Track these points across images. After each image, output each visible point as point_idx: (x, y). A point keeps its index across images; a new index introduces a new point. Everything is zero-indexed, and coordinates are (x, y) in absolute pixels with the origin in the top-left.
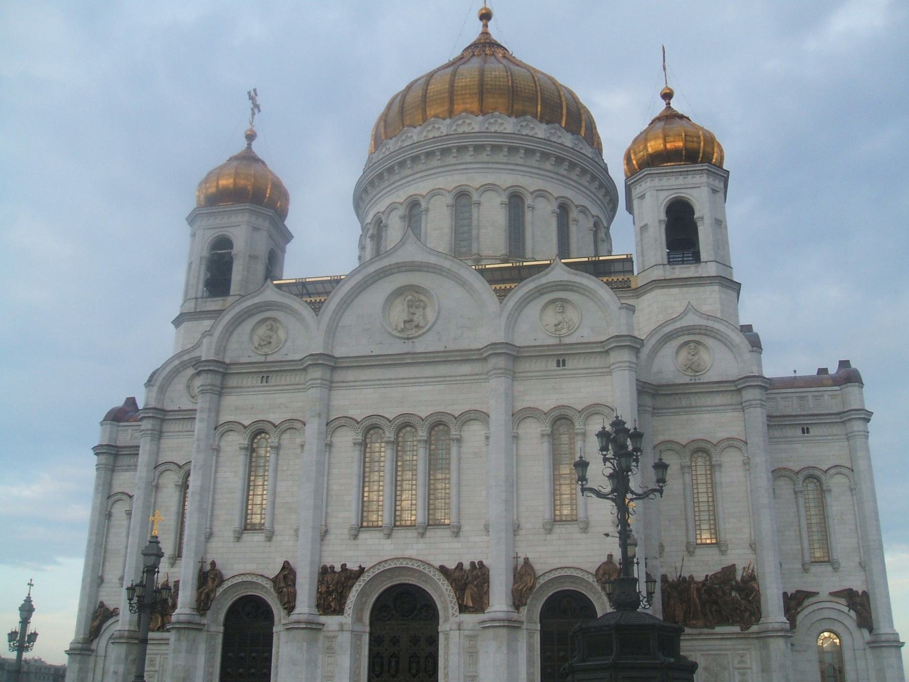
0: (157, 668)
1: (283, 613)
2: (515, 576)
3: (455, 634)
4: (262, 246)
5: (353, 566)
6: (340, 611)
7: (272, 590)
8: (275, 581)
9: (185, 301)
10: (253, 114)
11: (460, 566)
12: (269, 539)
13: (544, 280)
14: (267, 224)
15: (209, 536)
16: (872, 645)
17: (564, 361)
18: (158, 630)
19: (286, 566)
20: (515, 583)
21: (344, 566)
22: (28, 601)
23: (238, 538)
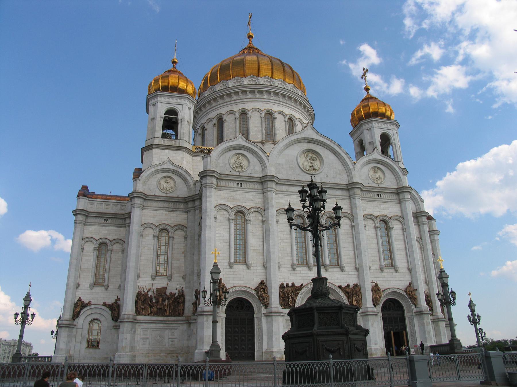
0: (148, 336)
1: (263, 307)
2: (372, 291)
5: (297, 284)
7: (255, 295)
8: (256, 290)
11: (348, 286)
12: (248, 268)
13: (371, 157)
17: (380, 195)
18: (148, 315)
19: (262, 283)
20: (373, 295)
21: (293, 284)
22: (28, 295)
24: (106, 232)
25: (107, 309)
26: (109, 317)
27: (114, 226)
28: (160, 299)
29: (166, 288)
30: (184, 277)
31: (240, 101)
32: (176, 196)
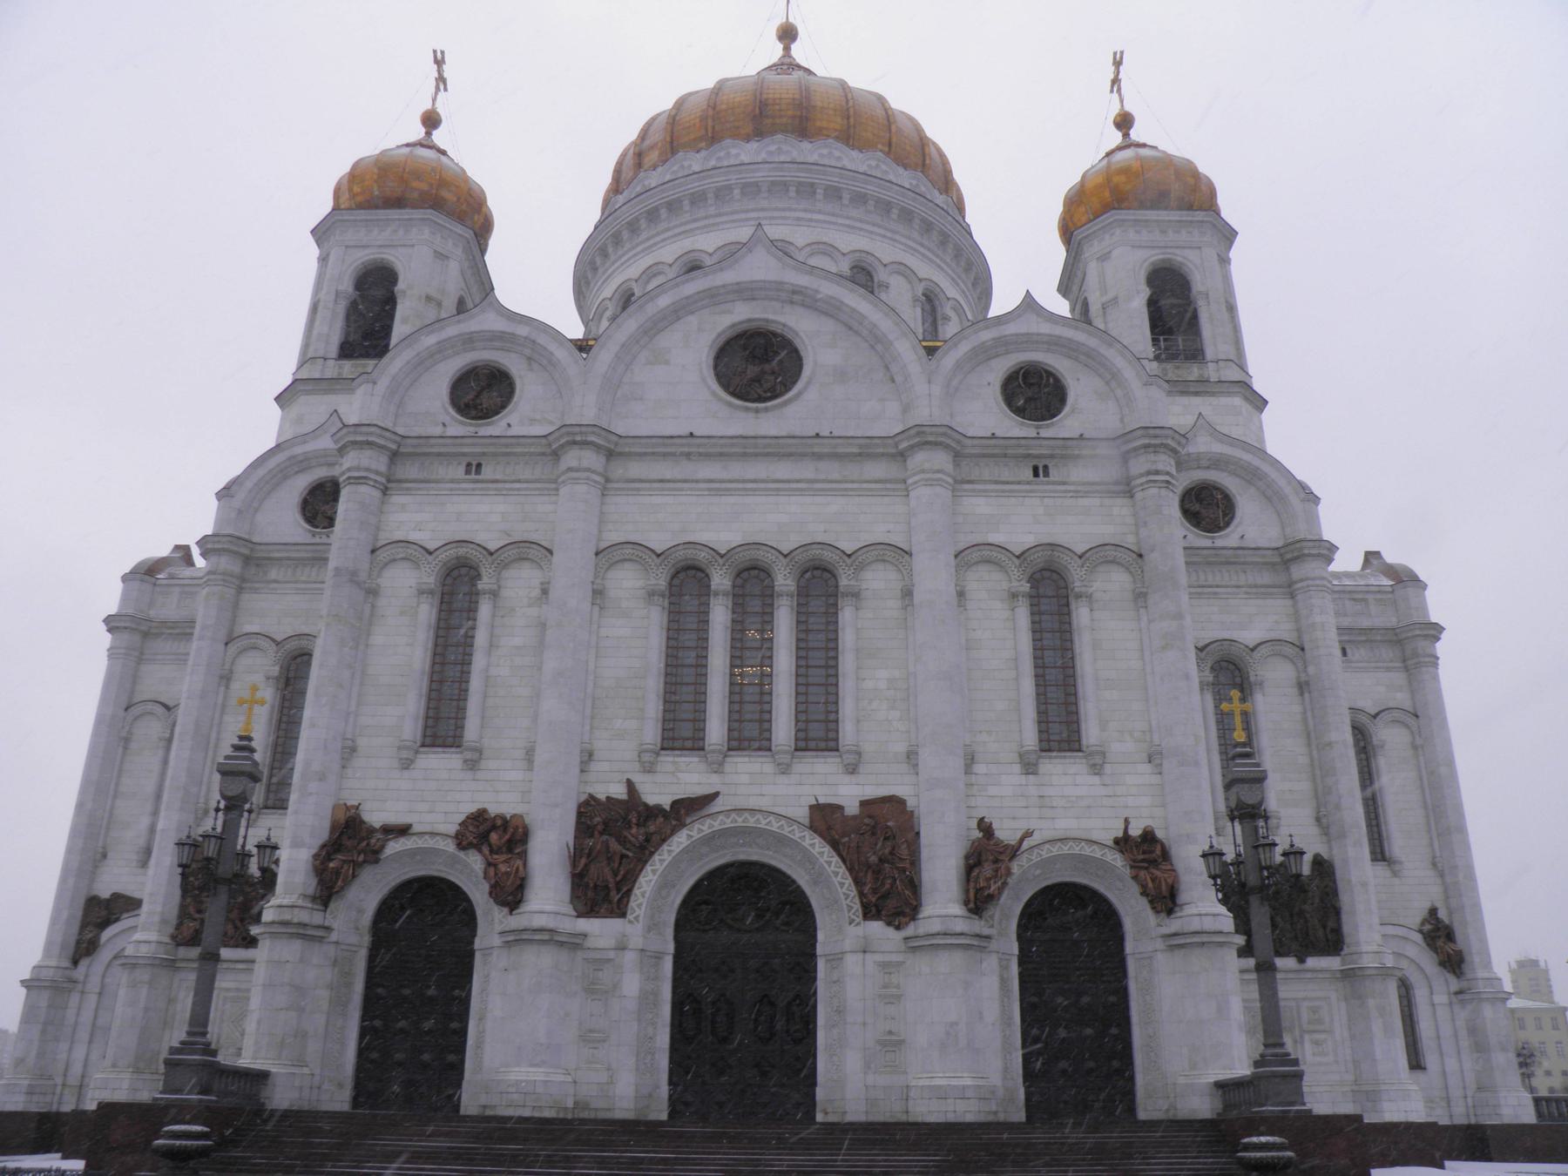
3: (852, 963)
4: (452, 281)
6: (620, 911)
9: (301, 365)
10: (438, 89)
12: (472, 765)
14: (459, 252)
15: (350, 751)
16: (1460, 997)
17: (1046, 467)
23: (407, 765)
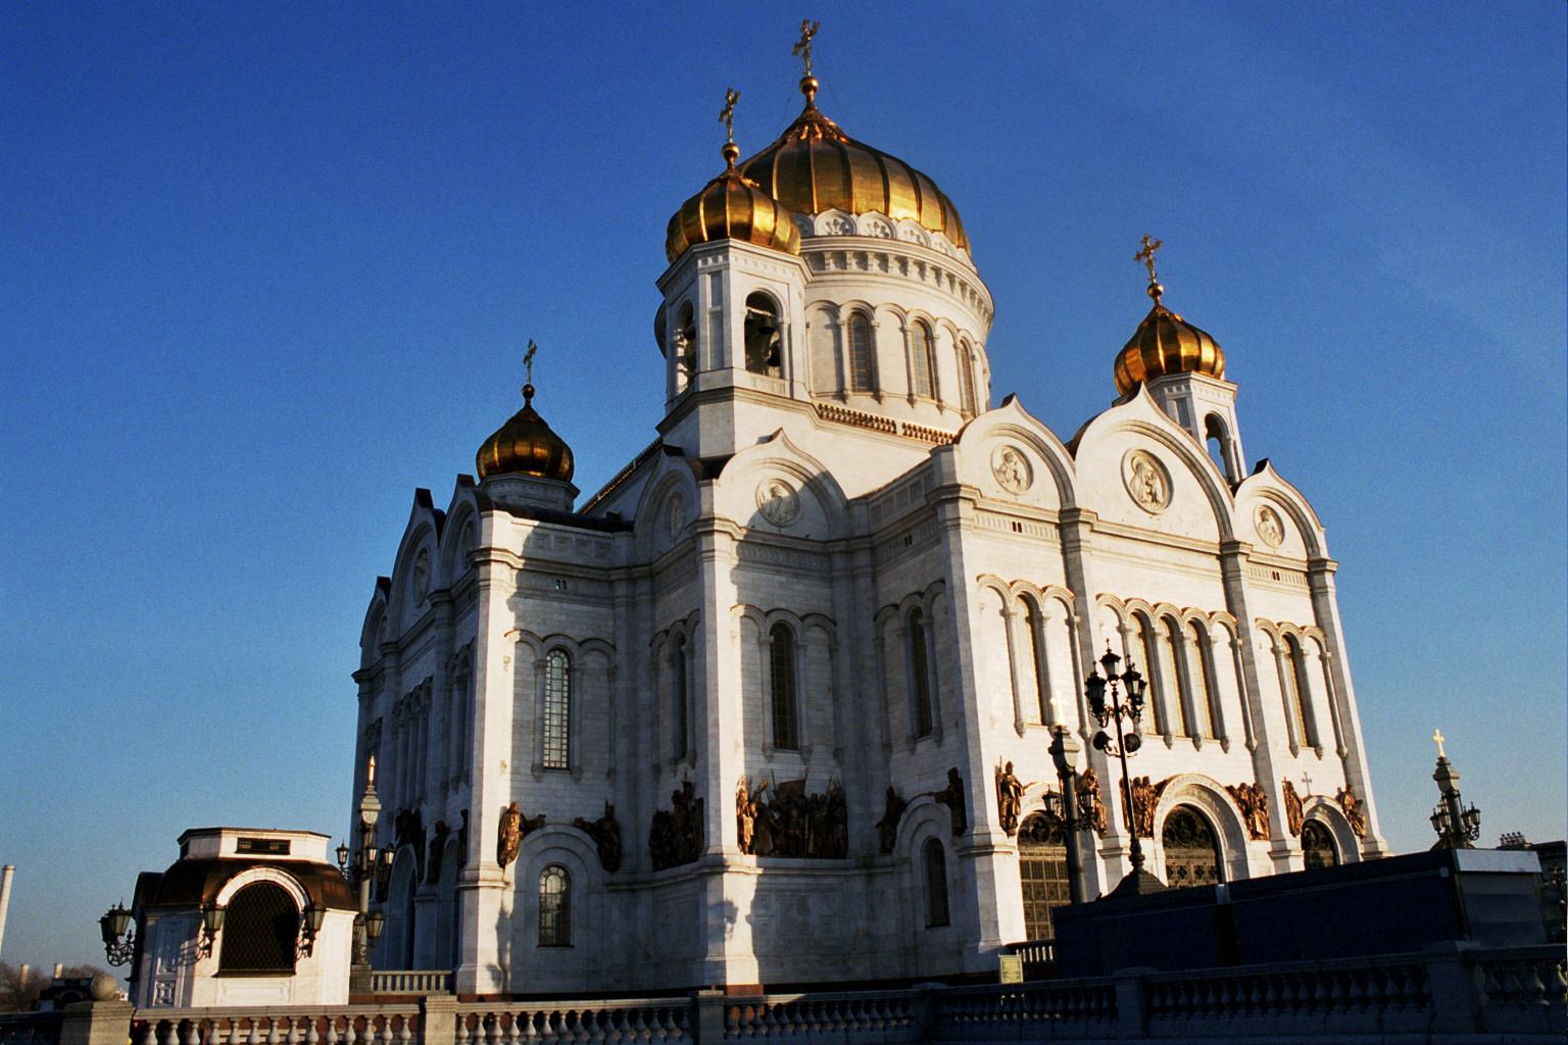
24: (563, 618)
25: (587, 838)
26: (593, 860)
27: (581, 603)
28: (795, 813)
29: (804, 782)
30: (838, 753)
31: (846, 277)
32: (804, 536)
